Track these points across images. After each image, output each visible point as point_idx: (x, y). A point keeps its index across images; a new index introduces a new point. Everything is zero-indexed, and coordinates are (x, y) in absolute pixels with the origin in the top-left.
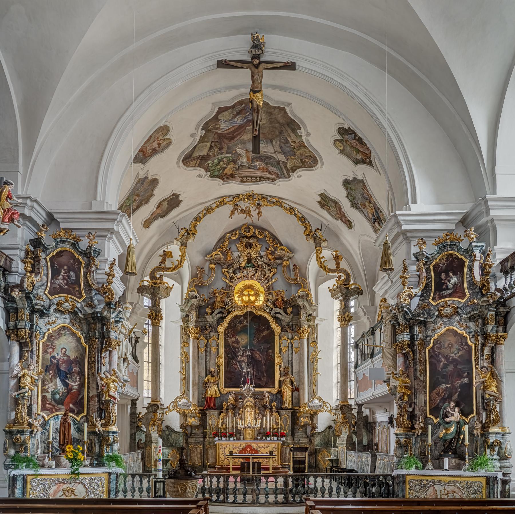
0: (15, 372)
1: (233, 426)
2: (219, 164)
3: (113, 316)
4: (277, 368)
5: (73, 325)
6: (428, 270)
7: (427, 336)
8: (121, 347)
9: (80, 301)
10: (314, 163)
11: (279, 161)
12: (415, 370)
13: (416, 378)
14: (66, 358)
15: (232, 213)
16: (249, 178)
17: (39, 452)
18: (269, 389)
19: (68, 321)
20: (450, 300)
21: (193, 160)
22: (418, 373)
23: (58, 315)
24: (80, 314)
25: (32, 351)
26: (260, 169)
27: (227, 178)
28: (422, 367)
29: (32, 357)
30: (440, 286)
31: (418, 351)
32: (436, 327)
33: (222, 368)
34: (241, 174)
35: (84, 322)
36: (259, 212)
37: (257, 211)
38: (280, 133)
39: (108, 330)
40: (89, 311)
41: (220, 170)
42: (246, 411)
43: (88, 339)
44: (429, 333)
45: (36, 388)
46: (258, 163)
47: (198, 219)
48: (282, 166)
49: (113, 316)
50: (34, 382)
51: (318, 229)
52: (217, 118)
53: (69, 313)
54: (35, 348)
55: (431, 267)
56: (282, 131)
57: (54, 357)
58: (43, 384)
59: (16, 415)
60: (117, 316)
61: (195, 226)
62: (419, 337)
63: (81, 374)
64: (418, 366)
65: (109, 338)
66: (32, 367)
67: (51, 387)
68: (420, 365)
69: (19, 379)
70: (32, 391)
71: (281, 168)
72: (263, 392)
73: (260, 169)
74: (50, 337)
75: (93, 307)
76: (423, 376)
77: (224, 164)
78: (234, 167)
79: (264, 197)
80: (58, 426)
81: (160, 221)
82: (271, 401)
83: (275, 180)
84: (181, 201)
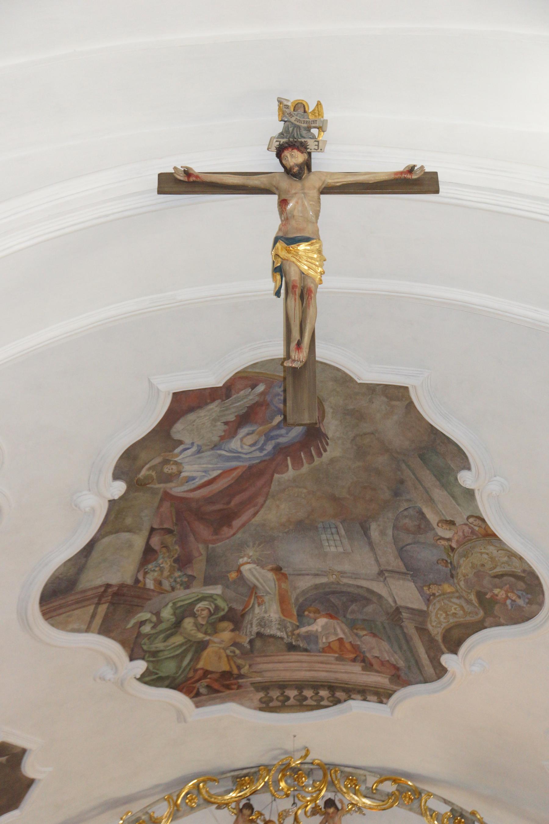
2: (178, 624)
10: (530, 602)
11: (398, 610)
16: (292, 693)
21: (81, 602)
26: (327, 649)
27: (212, 690)
34: (260, 672)
38: (396, 494)
41: (181, 657)
46: (322, 621)
48: (410, 628)
52: (168, 436)
56: (402, 482)
71: (408, 639)
73: (327, 649)
77: (198, 626)
78: (235, 644)
83: (389, 696)
84: (30, 783)
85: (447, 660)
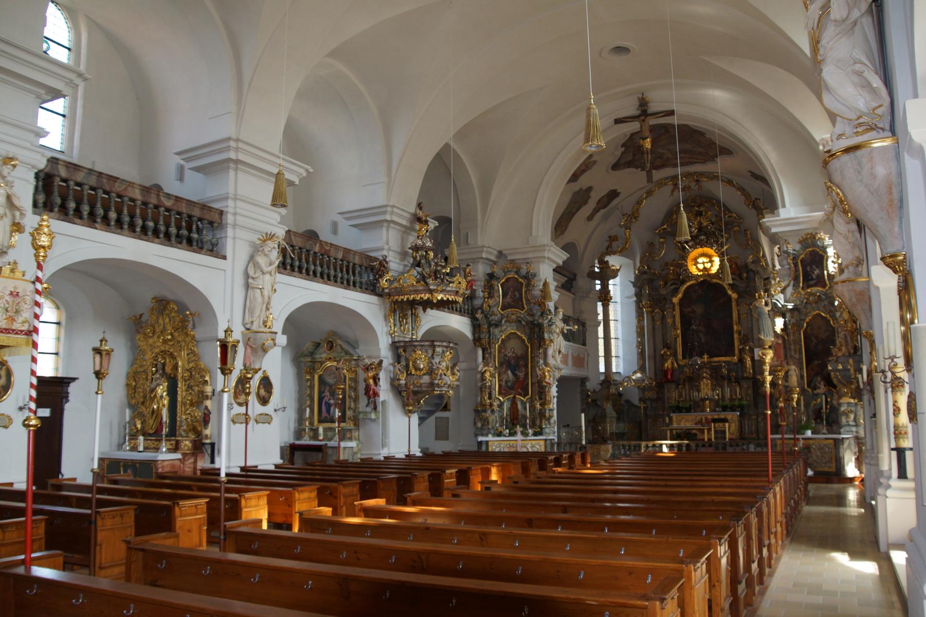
0: (480, 369)
1: (690, 396)
3: (546, 322)
4: (736, 336)
5: (519, 331)
6: (796, 265)
7: (801, 320)
8: (555, 343)
9: (523, 312)
12: (790, 349)
13: (791, 356)
14: (514, 355)
15: (673, 191)
17: (497, 425)
18: (728, 359)
19: (515, 328)
20: (814, 289)
22: (793, 352)
23: (507, 324)
24: (523, 322)
25: (490, 353)
28: (797, 347)
29: (491, 358)
30: (807, 278)
31: (791, 333)
32: (807, 311)
33: (679, 340)
35: (527, 327)
36: (699, 186)
37: (697, 186)
39: (543, 333)
40: (530, 319)
42: (702, 383)
43: (530, 339)
44: (803, 317)
45: (494, 379)
47: (639, 203)
49: (546, 322)
50: (492, 376)
51: (756, 199)
53: (515, 322)
54: (492, 350)
55: (799, 261)
57: (506, 355)
58: (499, 376)
59: (481, 399)
60: (550, 321)
61: (637, 210)
62: (792, 322)
63: (526, 366)
64: (792, 347)
65: (544, 339)
66: (490, 365)
67: (505, 378)
68: (795, 345)
69: (483, 374)
70: (491, 381)
72: (719, 362)
74: (503, 340)
75: (532, 315)
76: (798, 354)
79: (701, 174)
80: (509, 406)
81: (602, 211)
82: (729, 371)
85: (716, 159)
